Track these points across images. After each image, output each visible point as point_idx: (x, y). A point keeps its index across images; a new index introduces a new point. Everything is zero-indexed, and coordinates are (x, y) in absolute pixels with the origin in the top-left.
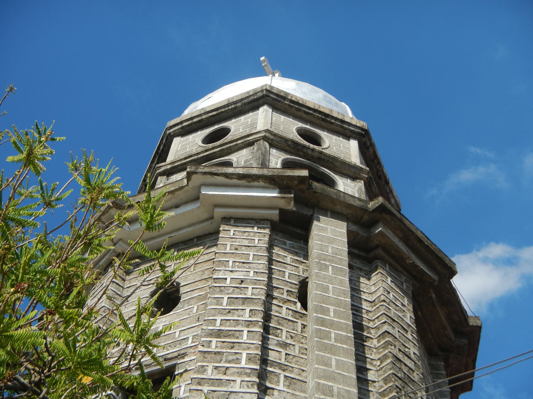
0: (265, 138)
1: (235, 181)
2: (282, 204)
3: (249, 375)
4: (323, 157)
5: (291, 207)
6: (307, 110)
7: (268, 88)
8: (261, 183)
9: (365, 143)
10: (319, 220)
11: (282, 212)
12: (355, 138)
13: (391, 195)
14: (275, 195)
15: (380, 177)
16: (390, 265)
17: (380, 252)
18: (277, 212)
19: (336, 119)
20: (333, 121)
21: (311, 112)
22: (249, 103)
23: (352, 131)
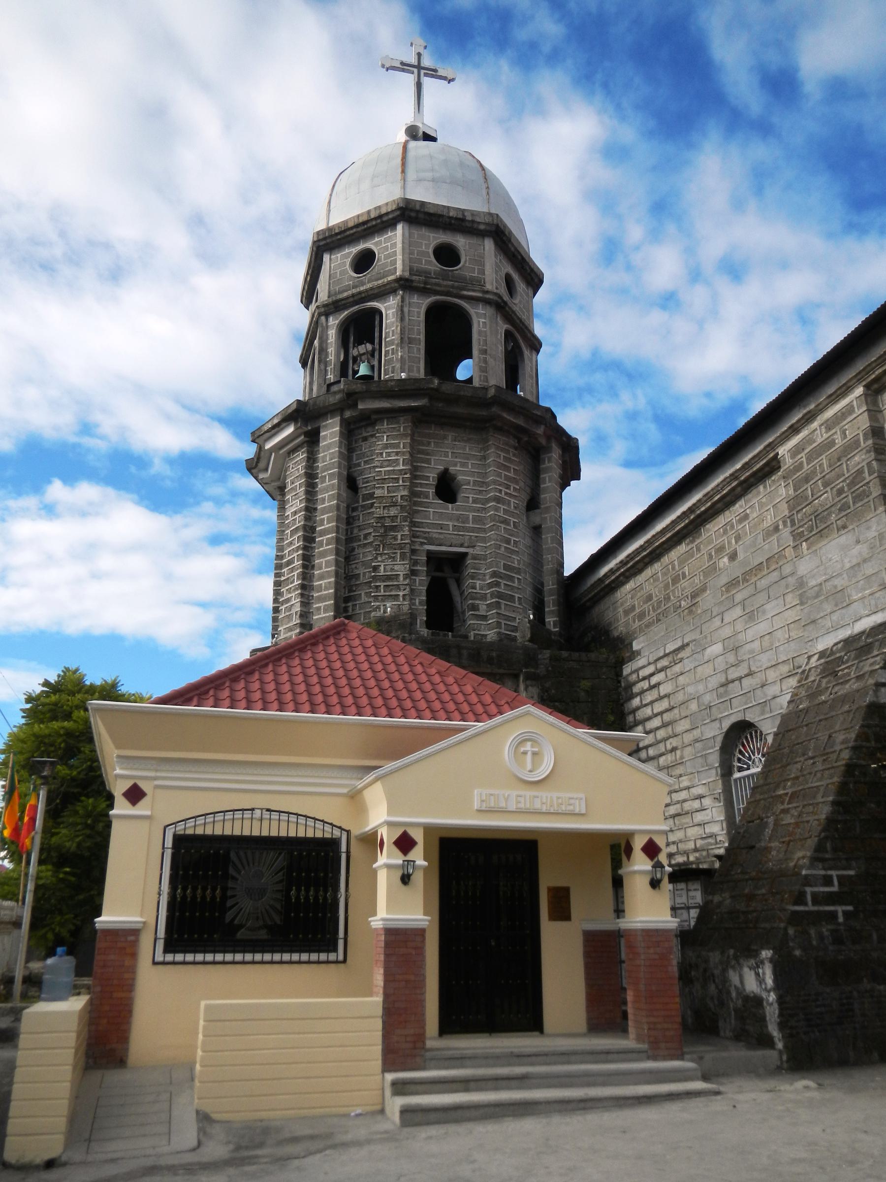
0: (320, 315)
1: (273, 431)
2: (300, 431)
3: (297, 589)
4: (363, 295)
5: (305, 429)
6: (352, 232)
7: (315, 239)
8: (284, 424)
9: (410, 217)
10: (326, 426)
11: (306, 434)
12: (399, 221)
13: (475, 226)
14: (290, 430)
15: (450, 224)
16: (387, 418)
17: (374, 417)
18: (303, 437)
19: (375, 219)
20: (374, 223)
21: (354, 230)
22: (316, 257)
23: (394, 219)
